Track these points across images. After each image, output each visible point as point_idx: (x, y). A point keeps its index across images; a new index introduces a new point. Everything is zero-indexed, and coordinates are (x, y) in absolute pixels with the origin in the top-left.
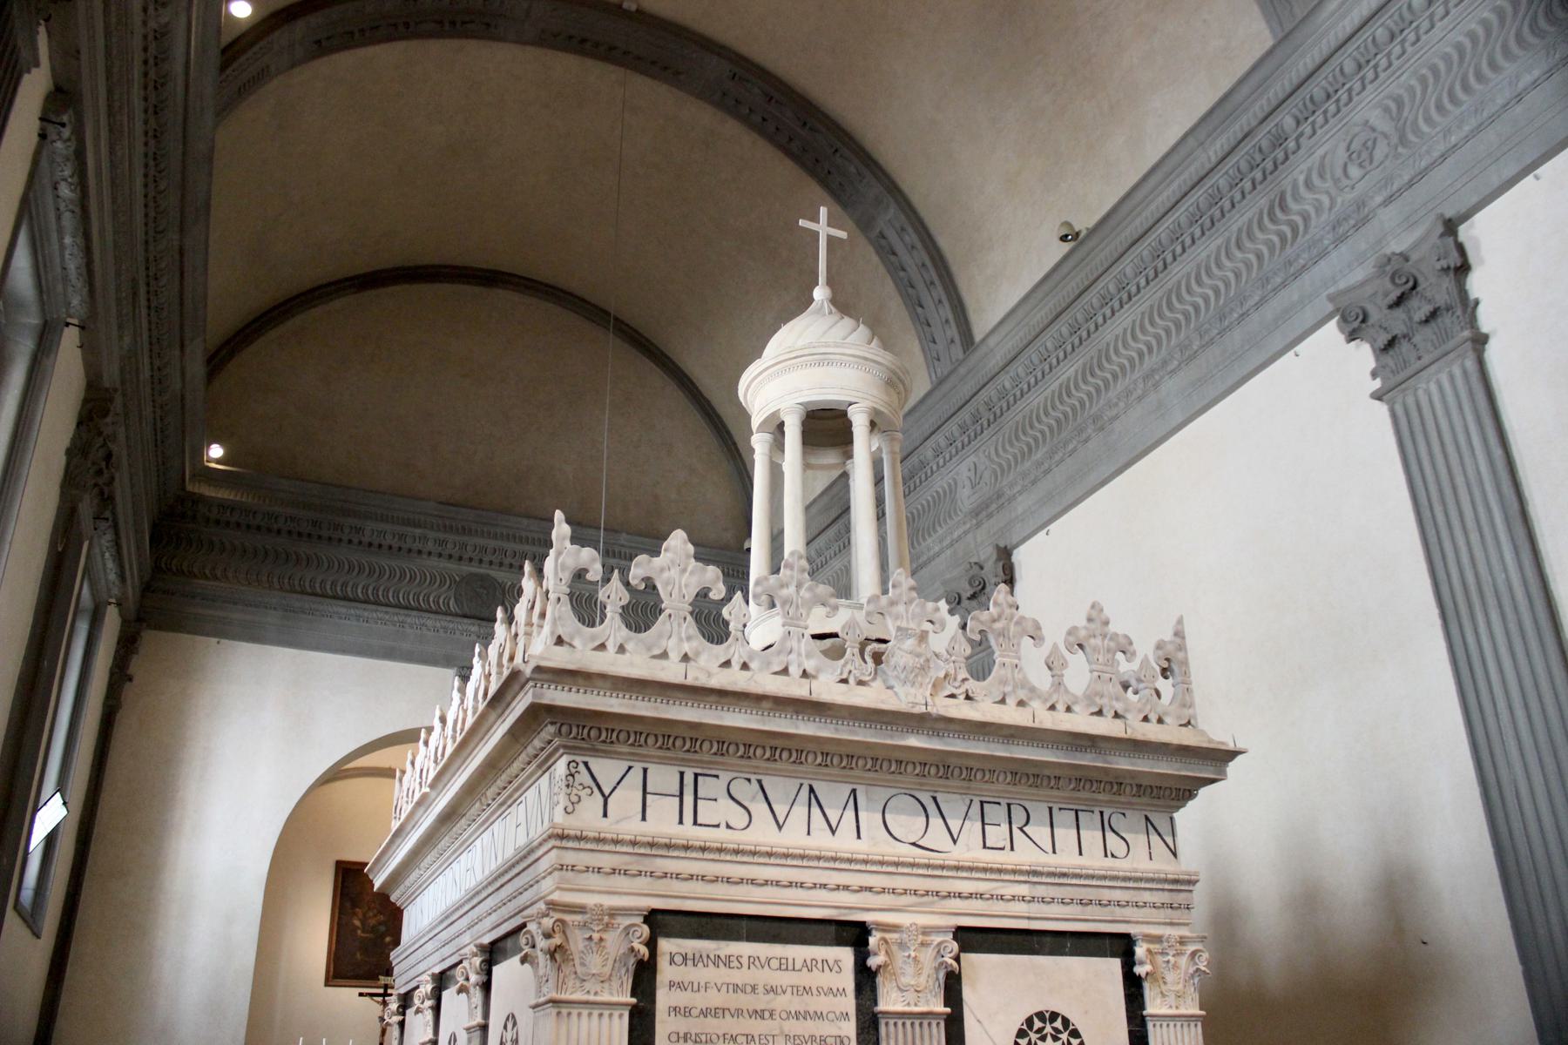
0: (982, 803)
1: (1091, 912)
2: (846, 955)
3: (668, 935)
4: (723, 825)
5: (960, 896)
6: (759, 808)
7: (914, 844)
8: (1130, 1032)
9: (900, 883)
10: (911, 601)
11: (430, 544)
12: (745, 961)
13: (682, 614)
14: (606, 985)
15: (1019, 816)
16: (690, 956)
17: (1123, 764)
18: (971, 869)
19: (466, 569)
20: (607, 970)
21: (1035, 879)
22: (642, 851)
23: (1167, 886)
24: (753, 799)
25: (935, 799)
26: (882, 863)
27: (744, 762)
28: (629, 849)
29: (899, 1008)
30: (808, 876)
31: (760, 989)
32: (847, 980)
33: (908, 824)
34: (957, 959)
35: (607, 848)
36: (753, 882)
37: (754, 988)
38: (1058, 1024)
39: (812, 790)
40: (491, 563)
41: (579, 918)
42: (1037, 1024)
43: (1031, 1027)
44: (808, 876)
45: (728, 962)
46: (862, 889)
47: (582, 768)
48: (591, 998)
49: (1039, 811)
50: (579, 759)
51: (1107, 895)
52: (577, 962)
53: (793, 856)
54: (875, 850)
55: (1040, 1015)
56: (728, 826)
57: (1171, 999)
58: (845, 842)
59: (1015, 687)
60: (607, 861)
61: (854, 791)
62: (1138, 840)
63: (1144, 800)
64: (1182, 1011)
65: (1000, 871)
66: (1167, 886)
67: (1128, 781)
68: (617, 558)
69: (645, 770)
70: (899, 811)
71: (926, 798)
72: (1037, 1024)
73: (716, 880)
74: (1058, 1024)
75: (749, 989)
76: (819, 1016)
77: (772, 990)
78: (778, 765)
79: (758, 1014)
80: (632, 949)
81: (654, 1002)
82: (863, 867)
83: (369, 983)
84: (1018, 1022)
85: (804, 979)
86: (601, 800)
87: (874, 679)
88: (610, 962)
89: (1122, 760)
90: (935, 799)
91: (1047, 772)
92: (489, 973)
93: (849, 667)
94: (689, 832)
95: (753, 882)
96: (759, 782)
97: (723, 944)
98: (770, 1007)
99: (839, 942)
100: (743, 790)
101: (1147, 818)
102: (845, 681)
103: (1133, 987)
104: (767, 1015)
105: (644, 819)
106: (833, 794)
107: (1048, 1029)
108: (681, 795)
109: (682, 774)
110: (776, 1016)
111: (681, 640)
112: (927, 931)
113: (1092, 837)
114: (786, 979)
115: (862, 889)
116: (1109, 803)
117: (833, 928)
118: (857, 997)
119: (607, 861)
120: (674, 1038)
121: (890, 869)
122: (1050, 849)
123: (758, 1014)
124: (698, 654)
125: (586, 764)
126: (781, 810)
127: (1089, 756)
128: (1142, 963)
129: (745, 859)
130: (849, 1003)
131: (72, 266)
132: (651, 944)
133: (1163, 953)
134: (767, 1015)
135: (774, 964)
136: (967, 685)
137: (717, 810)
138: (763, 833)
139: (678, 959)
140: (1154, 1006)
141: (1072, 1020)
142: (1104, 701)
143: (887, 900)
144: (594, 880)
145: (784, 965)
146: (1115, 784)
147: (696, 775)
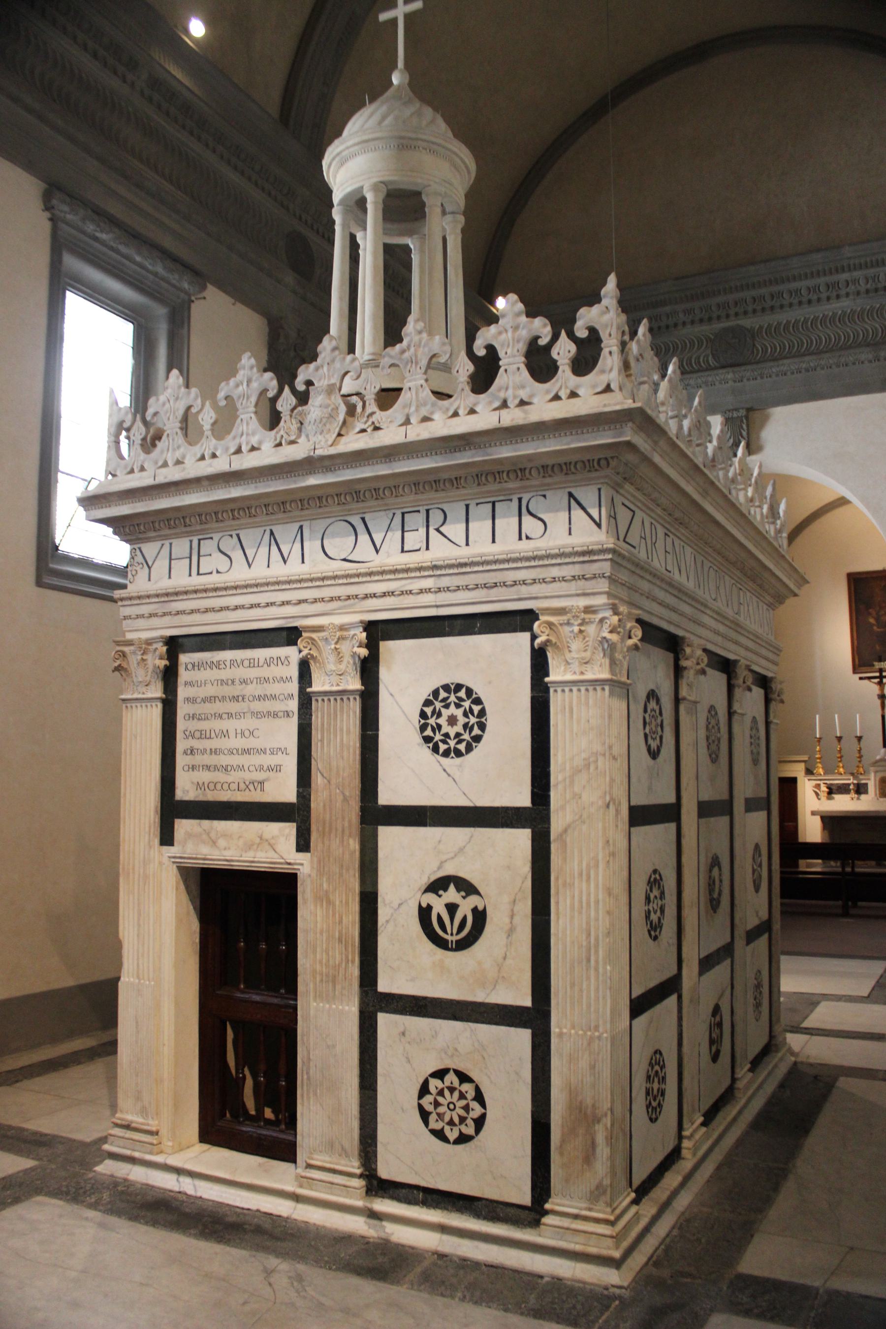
0: (403, 514)
1: (494, 594)
3: (184, 652)
4: (215, 572)
5: (374, 596)
6: (237, 555)
7: (345, 560)
8: (533, 698)
9: (327, 593)
10: (333, 361)
11: (681, 315)
12: (228, 663)
13: (174, 431)
15: (436, 518)
16: (196, 664)
17: (505, 452)
18: (383, 573)
19: (718, 326)
21: (439, 572)
22: (163, 599)
23: (577, 559)
24: (233, 549)
25: (363, 519)
26: (311, 580)
27: (221, 525)
28: (156, 600)
29: (327, 688)
30: (262, 598)
31: (237, 682)
33: (340, 544)
35: (144, 601)
37: (233, 682)
38: (462, 694)
39: (272, 533)
40: (736, 314)
42: (443, 694)
43: (436, 699)
44: (262, 598)
45: (217, 665)
46: (300, 602)
48: (140, 696)
49: (456, 510)
50: (136, 546)
52: (134, 674)
53: (262, 585)
54: (315, 570)
55: (446, 688)
56: (218, 572)
57: (575, 666)
58: (295, 568)
59: (418, 407)
60: (145, 609)
61: (301, 527)
62: (557, 520)
63: (556, 479)
64: (589, 676)
65: (407, 570)
66: (577, 559)
67: (529, 465)
68: (563, 322)
69: (171, 544)
70: (333, 536)
71: (356, 521)
72: (443, 694)
73: (207, 611)
74: (462, 694)
75: (230, 682)
76: (274, 697)
77: (244, 682)
78: (242, 521)
79: (235, 699)
81: (176, 696)
82: (299, 585)
83: (869, 669)
85: (265, 672)
87: (299, 436)
88: (149, 673)
89: (505, 448)
90: (363, 519)
91: (445, 476)
93: (282, 432)
94: (197, 581)
95: (227, 608)
96: (238, 535)
98: (241, 693)
100: (229, 544)
101: (571, 495)
102: (280, 444)
104: (240, 698)
105: (170, 577)
106: (286, 533)
107: (453, 698)
108: (190, 558)
109: (191, 541)
110: (246, 700)
111: (174, 450)
112: (342, 628)
113: (507, 524)
114: (253, 673)
115: (300, 602)
116: (526, 489)
117: (284, 634)
118: (299, 683)
119: (145, 609)
120: (187, 718)
121: (318, 583)
122: (463, 542)
123: (235, 699)
124: (184, 457)
125: (140, 549)
126: (250, 553)
127: (469, 453)
129: (221, 593)
130: (294, 687)
131: (159, 269)
133: (568, 623)
134: (240, 698)
135: (246, 663)
136: (374, 418)
137: (213, 561)
138: (240, 573)
139: (190, 666)
140: (556, 674)
142: (510, 394)
144: (141, 623)
145: (253, 664)
146: (519, 470)
147: (199, 540)
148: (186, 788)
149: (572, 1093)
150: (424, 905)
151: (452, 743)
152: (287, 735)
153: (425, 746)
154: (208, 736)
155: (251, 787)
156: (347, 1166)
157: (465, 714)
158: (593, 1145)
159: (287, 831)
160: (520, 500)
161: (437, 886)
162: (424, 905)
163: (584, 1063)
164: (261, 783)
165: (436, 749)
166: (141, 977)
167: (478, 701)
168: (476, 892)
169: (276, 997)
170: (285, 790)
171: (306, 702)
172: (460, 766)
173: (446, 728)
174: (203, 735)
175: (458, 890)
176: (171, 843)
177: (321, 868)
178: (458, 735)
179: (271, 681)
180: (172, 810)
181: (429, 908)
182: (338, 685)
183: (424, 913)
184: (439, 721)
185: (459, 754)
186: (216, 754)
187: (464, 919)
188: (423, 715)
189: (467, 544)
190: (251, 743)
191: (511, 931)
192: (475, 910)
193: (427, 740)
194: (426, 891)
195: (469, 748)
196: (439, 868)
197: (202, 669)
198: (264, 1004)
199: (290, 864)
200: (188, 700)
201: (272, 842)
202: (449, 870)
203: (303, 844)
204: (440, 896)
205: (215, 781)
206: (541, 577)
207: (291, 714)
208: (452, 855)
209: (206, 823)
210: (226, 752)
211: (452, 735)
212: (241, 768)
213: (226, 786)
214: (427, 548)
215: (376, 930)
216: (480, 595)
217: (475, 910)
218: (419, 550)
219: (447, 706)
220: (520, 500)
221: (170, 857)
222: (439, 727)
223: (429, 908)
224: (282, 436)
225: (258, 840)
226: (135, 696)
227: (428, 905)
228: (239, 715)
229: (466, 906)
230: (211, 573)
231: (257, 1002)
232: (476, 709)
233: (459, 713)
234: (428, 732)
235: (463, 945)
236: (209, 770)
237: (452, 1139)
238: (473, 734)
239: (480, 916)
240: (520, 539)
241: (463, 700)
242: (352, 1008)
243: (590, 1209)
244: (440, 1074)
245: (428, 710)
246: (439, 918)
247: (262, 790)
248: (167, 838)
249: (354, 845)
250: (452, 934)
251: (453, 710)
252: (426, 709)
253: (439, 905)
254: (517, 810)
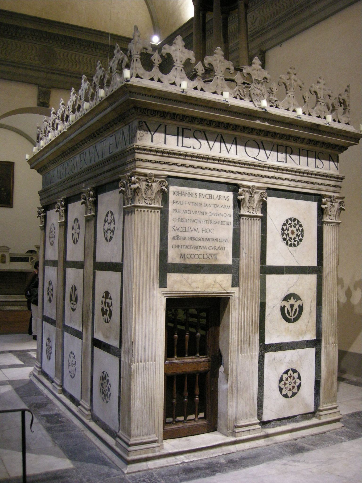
2: (230, 195)
4: (192, 147)
7: (254, 158)
8: (318, 226)
12: (198, 195)
14: (153, 201)
20: (153, 197)
26: (245, 164)
32: (231, 203)
34: (266, 198)
36: (201, 168)
38: (296, 222)
41: (144, 178)
42: (289, 222)
45: (192, 195)
47: (144, 123)
51: (315, 180)
55: (290, 219)
56: (194, 148)
72: (289, 222)
74: (296, 222)
76: (221, 215)
77: (207, 205)
79: (202, 213)
80: (162, 189)
81: (168, 208)
84: (283, 221)
86: (150, 136)
88: (154, 194)
92: (97, 197)
94: (180, 149)
95: (201, 168)
97: (191, 189)
99: (229, 190)
102: (235, 98)
103: (321, 212)
104: (205, 213)
109: (178, 128)
110: (208, 214)
118: (233, 209)
120: (175, 220)
123: (202, 213)
128: (324, 204)
130: (231, 211)
132: (167, 187)
136: (276, 103)
139: (176, 193)
141: (300, 221)
143: (245, 177)
148: (173, 257)
149: (327, 366)
150: (283, 306)
151: (293, 241)
152: (228, 233)
153: (283, 242)
154: (187, 230)
155: (210, 257)
156: (254, 421)
157: (297, 231)
158: (333, 383)
159: (227, 278)
160: (316, 152)
161: (287, 298)
163: (331, 355)
164: (215, 255)
165: (287, 243)
166: (147, 360)
167: (301, 226)
168: (300, 299)
169: (196, 358)
170: (226, 258)
171: (237, 218)
172: (295, 250)
173: (291, 235)
174: (184, 230)
176: (165, 287)
177: (245, 294)
178: (295, 238)
179: (220, 207)
180: (165, 268)
181: (284, 307)
182: (252, 213)
183: (283, 309)
184: (288, 232)
185: (295, 246)
186: (191, 240)
187: (296, 309)
188: (283, 229)
189: (299, 164)
190: (209, 235)
191: (311, 312)
193: (284, 239)
194: (283, 300)
195: (298, 244)
196: (288, 291)
197: (183, 195)
198: (193, 363)
199: (228, 293)
200: (175, 210)
201: (221, 283)
202: (291, 291)
203: (235, 283)
204: (288, 302)
205: (191, 253)
206: (324, 183)
207: (229, 224)
208: (292, 285)
209: (186, 275)
210: (197, 239)
211: (293, 238)
212: (205, 247)
213: (196, 256)
214: (286, 162)
215: (265, 318)
216: (305, 185)
218: (283, 162)
219: (291, 227)
220: (316, 152)
221: (163, 294)
222: (288, 234)
223: (284, 306)
224: (238, 94)
225: (213, 283)
226: (143, 205)
228: (204, 221)
230: (190, 147)
231: (189, 363)
232: (301, 228)
233: (295, 229)
234: (285, 236)
235: (295, 320)
236: (187, 248)
237: (290, 396)
238: (300, 238)
239: (301, 308)
240: (316, 167)
241: (296, 225)
242: (257, 353)
243: (332, 405)
244: (286, 372)
245: (285, 227)
246: (288, 310)
247: (216, 258)
248: (163, 284)
249: (258, 282)
251: (293, 228)
252: (284, 227)
254: (313, 267)
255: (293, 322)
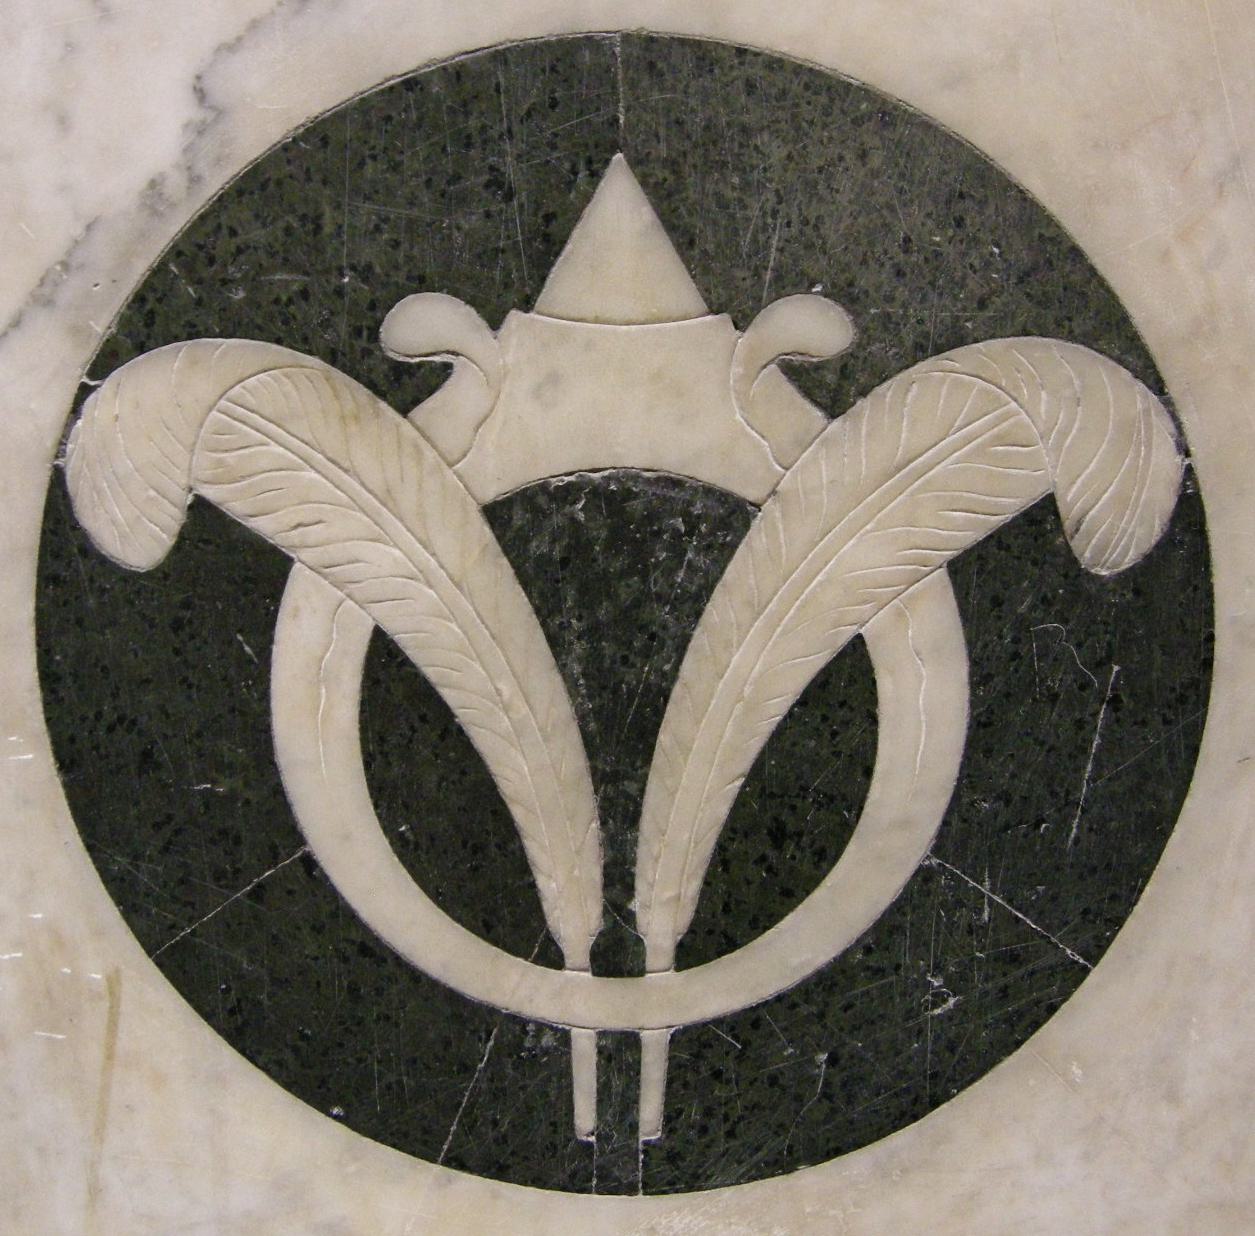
150: (135, 533)
162: (135, 533)
168: (1058, 292)
175: (732, 289)
181: (229, 573)
192: (1014, 575)
194: (152, 319)
204: (408, 385)
217: (1014, 575)
223: (229, 573)
227: (206, 525)
229: (854, 546)
246: (401, 709)
250: (616, 955)
253: (382, 538)
255: (676, 1169)
